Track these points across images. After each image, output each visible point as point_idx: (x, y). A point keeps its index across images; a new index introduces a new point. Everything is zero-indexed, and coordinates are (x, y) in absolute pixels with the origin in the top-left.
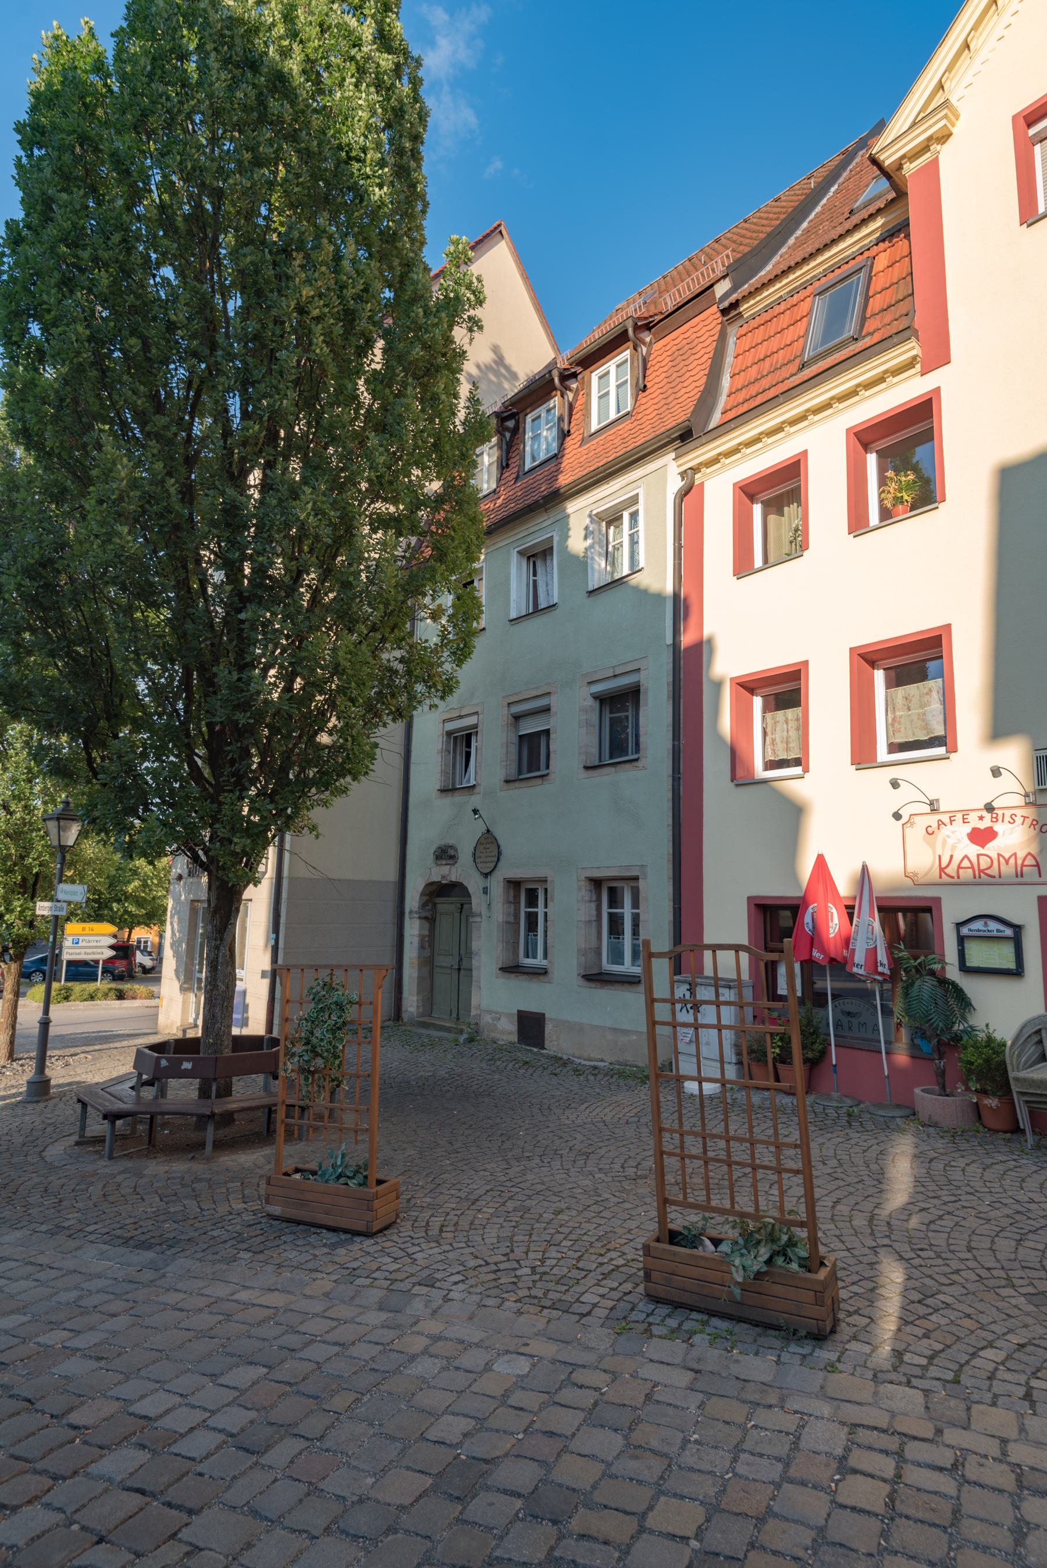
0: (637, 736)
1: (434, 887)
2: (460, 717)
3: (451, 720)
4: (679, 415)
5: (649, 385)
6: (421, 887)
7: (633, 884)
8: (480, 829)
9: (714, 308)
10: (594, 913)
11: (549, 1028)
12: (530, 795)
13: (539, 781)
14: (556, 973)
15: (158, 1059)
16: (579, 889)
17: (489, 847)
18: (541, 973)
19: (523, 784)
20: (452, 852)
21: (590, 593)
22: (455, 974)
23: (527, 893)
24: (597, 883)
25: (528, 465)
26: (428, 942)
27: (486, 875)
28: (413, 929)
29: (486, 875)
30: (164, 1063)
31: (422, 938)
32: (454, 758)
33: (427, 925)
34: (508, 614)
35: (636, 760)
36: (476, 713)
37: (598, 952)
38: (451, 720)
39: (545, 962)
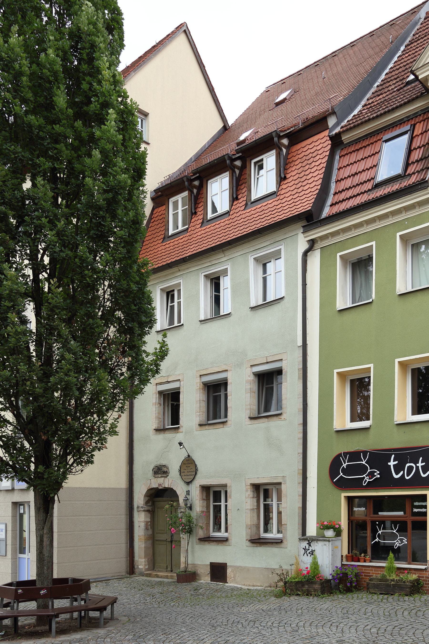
0: (257, 238)
1: (153, 491)
2: (168, 382)
3: (161, 384)
4: (305, 204)
5: (288, 176)
6: (144, 491)
7: (278, 487)
8: (183, 455)
9: (326, 133)
10: (256, 504)
11: (229, 571)
12: (213, 434)
13: (221, 426)
14: (233, 540)
15: (16, 590)
16: (247, 491)
17: (189, 467)
18: (225, 540)
19: (211, 427)
20: (165, 469)
21: (252, 308)
22: (169, 545)
23: (215, 494)
24: (256, 487)
25: (210, 215)
26: (152, 525)
27: (188, 483)
28: (141, 519)
29: (188, 483)
30: (20, 591)
31: (147, 523)
32: (164, 408)
33: (149, 515)
34: (199, 316)
35: (280, 414)
36: (179, 380)
37: (258, 526)
38: (161, 384)
39: (226, 535)
